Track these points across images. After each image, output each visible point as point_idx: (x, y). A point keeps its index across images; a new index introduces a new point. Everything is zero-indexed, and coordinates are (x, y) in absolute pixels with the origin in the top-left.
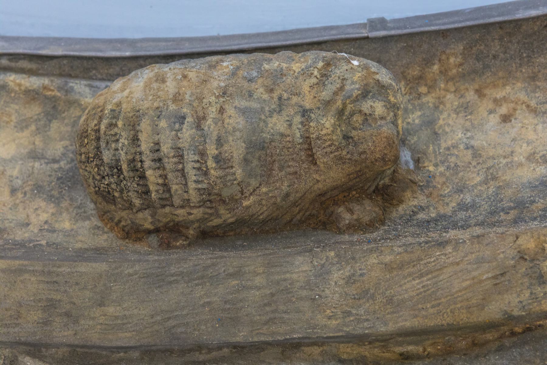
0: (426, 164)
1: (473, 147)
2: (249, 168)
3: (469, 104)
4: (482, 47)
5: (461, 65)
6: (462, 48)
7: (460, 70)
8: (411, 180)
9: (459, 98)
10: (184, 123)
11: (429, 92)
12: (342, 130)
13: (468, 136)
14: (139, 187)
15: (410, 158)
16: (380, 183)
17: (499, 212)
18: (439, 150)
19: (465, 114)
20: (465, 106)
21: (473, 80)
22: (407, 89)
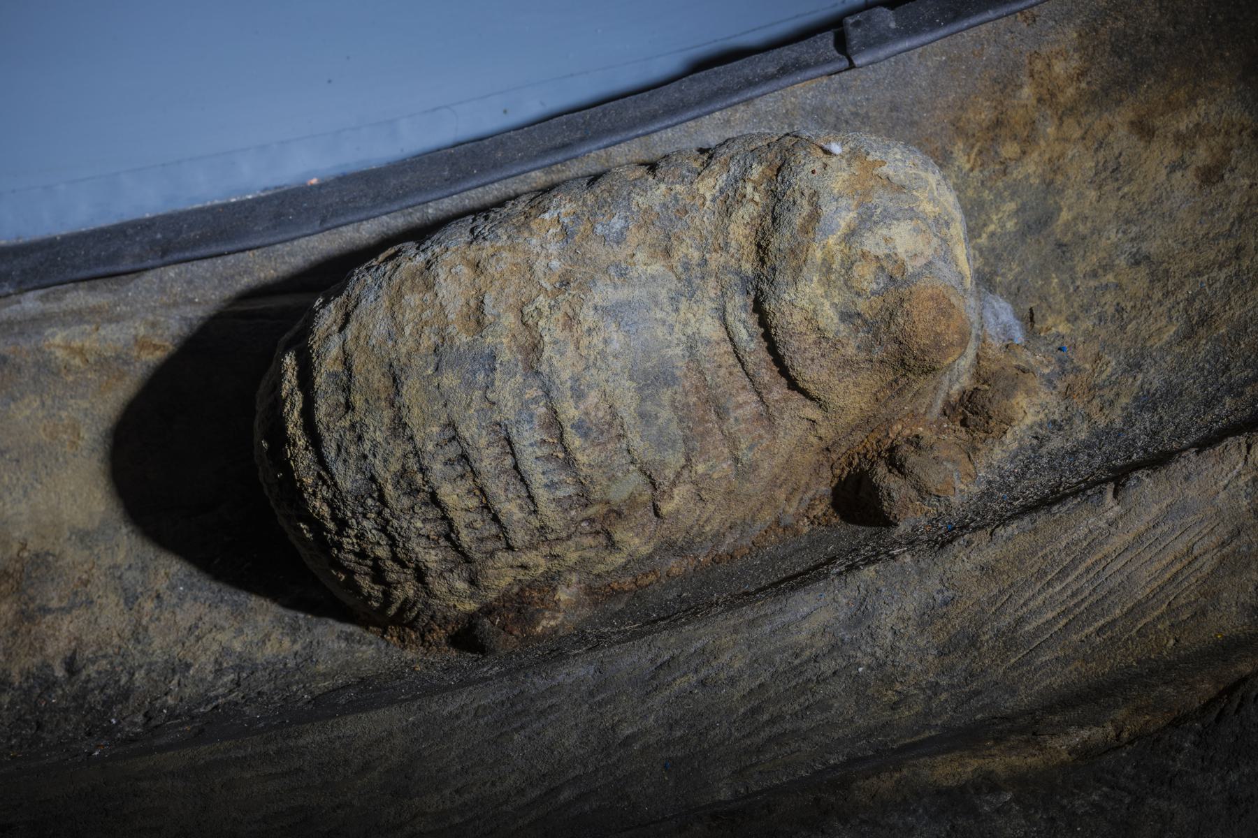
0: (1050, 321)
1: (1147, 257)
2: (654, 431)
3: (1121, 160)
4: (1120, 24)
5: (1082, 74)
6: (1075, 35)
7: (1083, 85)
8: (1018, 367)
9: (1097, 150)
10: (495, 369)
11: (1024, 153)
12: (834, 305)
13: (1133, 235)
14: (428, 526)
15: (1011, 316)
16: (952, 392)
17: (1222, 397)
18: (1073, 282)
19: (1116, 185)
20: (1111, 165)
21: (1119, 102)
22: (973, 156)
